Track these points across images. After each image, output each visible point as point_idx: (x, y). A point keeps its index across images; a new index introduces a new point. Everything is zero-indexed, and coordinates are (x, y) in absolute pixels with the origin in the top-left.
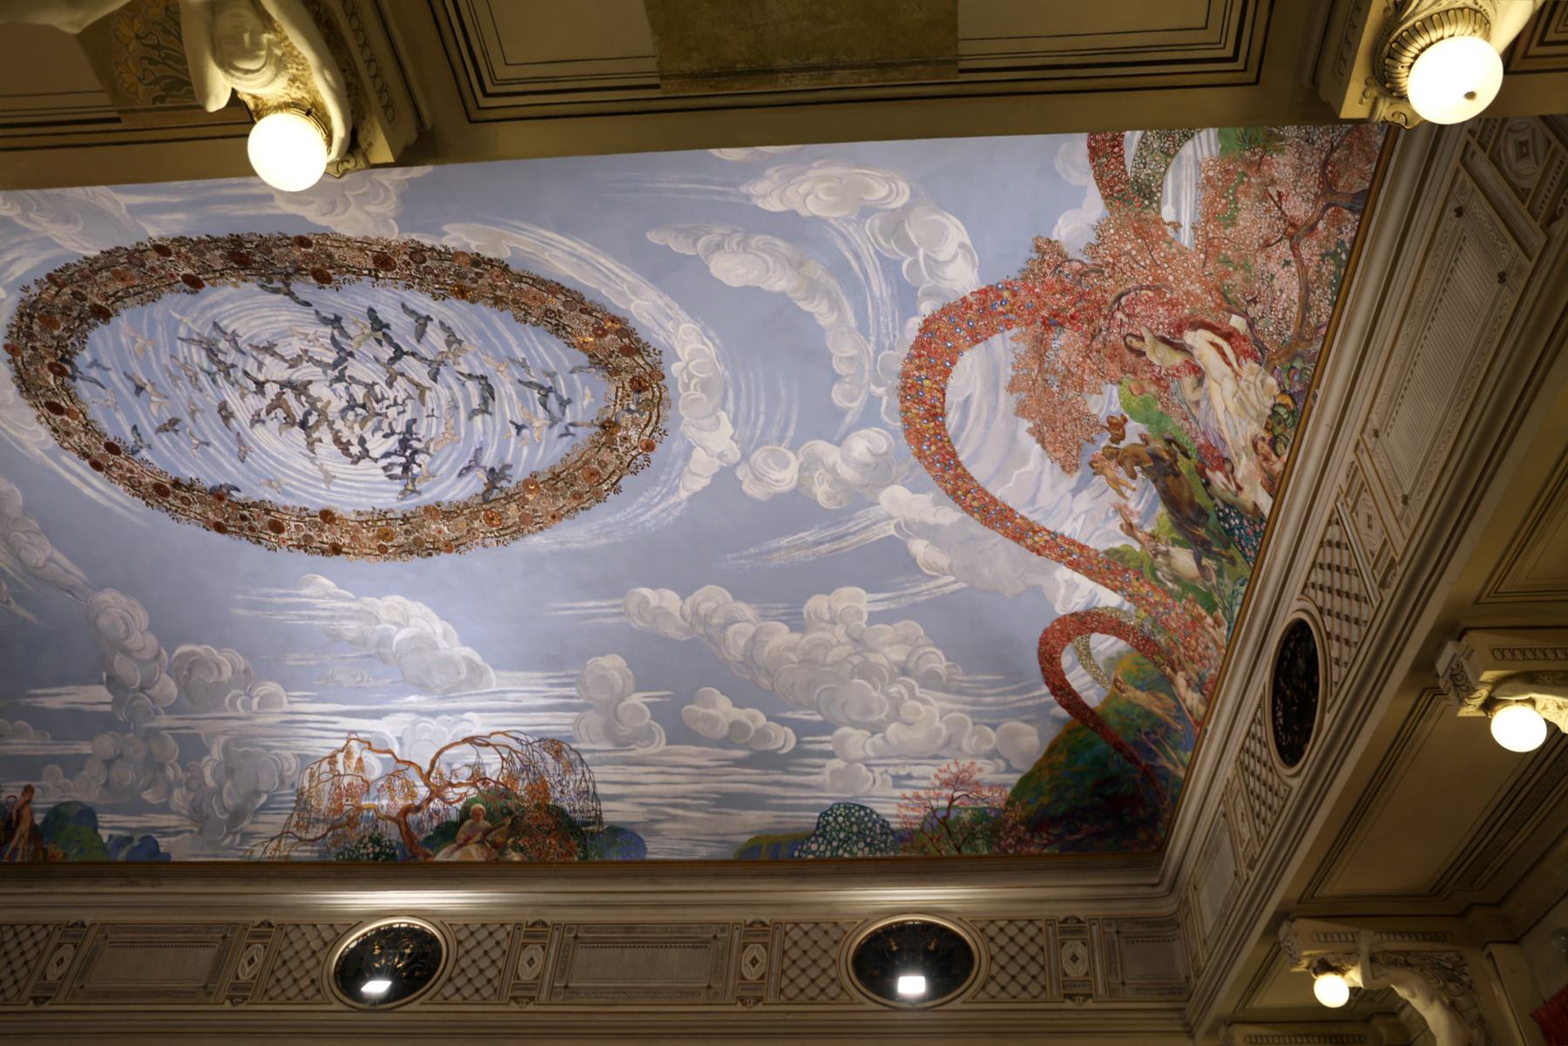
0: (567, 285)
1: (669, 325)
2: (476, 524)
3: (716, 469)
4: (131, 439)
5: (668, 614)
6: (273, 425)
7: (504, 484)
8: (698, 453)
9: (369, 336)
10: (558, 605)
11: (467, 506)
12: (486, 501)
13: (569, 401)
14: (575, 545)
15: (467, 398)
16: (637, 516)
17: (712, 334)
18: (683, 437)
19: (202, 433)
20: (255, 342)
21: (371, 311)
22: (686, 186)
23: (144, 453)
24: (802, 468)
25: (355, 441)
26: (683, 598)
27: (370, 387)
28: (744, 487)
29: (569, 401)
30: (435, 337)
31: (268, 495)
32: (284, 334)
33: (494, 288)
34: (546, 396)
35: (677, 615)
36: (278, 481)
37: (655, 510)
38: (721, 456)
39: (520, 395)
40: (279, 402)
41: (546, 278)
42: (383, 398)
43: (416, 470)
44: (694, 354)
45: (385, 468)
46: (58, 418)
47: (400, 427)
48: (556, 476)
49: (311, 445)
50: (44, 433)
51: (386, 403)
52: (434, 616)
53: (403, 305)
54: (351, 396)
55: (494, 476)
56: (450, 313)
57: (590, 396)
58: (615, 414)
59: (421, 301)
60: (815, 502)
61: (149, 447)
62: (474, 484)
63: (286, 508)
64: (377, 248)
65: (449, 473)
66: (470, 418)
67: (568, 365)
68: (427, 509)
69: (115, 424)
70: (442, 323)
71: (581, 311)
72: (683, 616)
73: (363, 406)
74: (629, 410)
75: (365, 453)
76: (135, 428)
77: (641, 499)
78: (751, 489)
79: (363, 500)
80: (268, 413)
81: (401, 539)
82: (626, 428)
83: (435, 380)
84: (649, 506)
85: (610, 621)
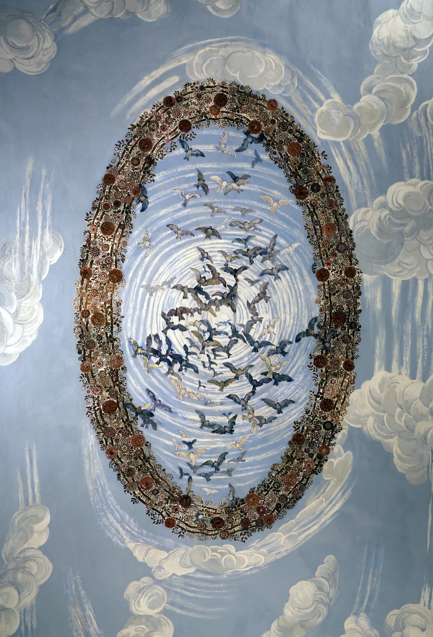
0: (299, 502)
1: (264, 550)
2: (106, 394)
3: (149, 565)
4: (196, 147)
5: (26, 539)
6: (200, 266)
7: (140, 421)
8: (164, 554)
9: (270, 369)
10: (34, 452)
11: (122, 390)
12: (125, 406)
13: (208, 480)
14: (87, 466)
15: (213, 413)
16: (112, 513)
17: (254, 572)
18: (177, 546)
19: (192, 206)
20: (269, 287)
21: (290, 380)
22: (369, 588)
23: (180, 151)
24: (148, 617)
25: (183, 323)
26: (40, 548)
27: (227, 350)
28: (134, 582)
29: (208, 480)
30: (266, 411)
31: (137, 234)
32: (275, 311)
33: (301, 460)
34: (213, 466)
35: (26, 546)
36: (151, 247)
37: (118, 526)
38: (160, 568)
39: (213, 451)
40: (217, 279)
41: (306, 492)
42: (216, 355)
43: (155, 359)
44: (241, 561)
45: (157, 336)
46: (212, 96)
47: (192, 359)
48: (147, 459)
49: (182, 289)
50: (200, 76)
51: (212, 356)
52: (23, 348)
53: (293, 402)
54: (219, 333)
55: (147, 415)
56: (283, 426)
57: (210, 493)
58: (196, 506)
59: (294, 414)
60: (122, 628)
61: (186, 158)
62: (141, 401)
63: (125, 244)
64: (338, 406)
65: (151, 384)
66: (197, 412)
67: (237, 485)
68: (120, 359)
69: (208, 140)
70: (275, 418)
71: (278, 504)
72: (24, 550)
73: (210, 339)
74: (198, 514)
75: (170, 326)
76: (202, 155)
77: (127, 517)
78: (132, 588)
79: (131, 311)
80: (209, 266)
81: (93, 331)
82: (184, 512)
83: (229, 397)
84: (121, 522)
85: (21, 495)
